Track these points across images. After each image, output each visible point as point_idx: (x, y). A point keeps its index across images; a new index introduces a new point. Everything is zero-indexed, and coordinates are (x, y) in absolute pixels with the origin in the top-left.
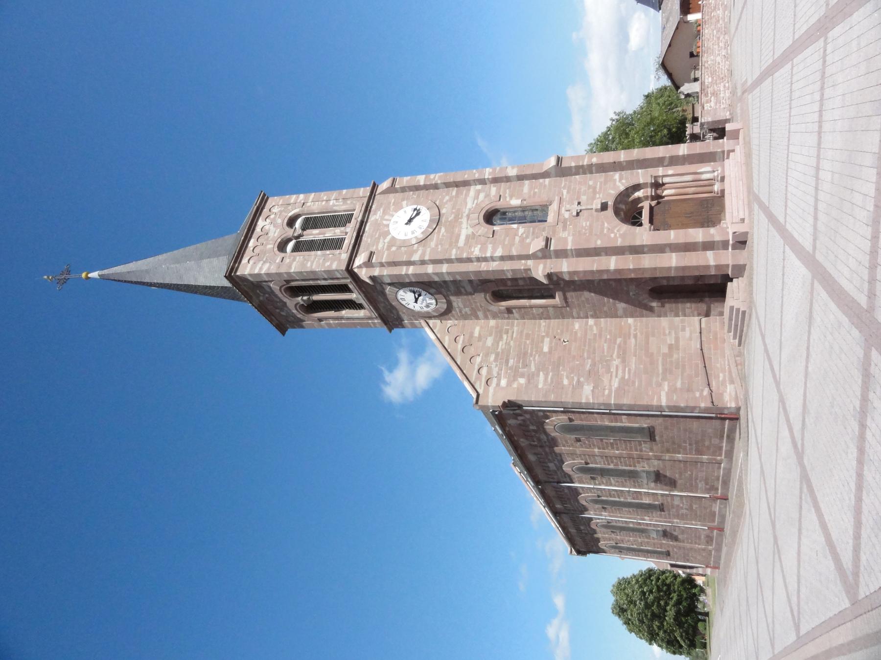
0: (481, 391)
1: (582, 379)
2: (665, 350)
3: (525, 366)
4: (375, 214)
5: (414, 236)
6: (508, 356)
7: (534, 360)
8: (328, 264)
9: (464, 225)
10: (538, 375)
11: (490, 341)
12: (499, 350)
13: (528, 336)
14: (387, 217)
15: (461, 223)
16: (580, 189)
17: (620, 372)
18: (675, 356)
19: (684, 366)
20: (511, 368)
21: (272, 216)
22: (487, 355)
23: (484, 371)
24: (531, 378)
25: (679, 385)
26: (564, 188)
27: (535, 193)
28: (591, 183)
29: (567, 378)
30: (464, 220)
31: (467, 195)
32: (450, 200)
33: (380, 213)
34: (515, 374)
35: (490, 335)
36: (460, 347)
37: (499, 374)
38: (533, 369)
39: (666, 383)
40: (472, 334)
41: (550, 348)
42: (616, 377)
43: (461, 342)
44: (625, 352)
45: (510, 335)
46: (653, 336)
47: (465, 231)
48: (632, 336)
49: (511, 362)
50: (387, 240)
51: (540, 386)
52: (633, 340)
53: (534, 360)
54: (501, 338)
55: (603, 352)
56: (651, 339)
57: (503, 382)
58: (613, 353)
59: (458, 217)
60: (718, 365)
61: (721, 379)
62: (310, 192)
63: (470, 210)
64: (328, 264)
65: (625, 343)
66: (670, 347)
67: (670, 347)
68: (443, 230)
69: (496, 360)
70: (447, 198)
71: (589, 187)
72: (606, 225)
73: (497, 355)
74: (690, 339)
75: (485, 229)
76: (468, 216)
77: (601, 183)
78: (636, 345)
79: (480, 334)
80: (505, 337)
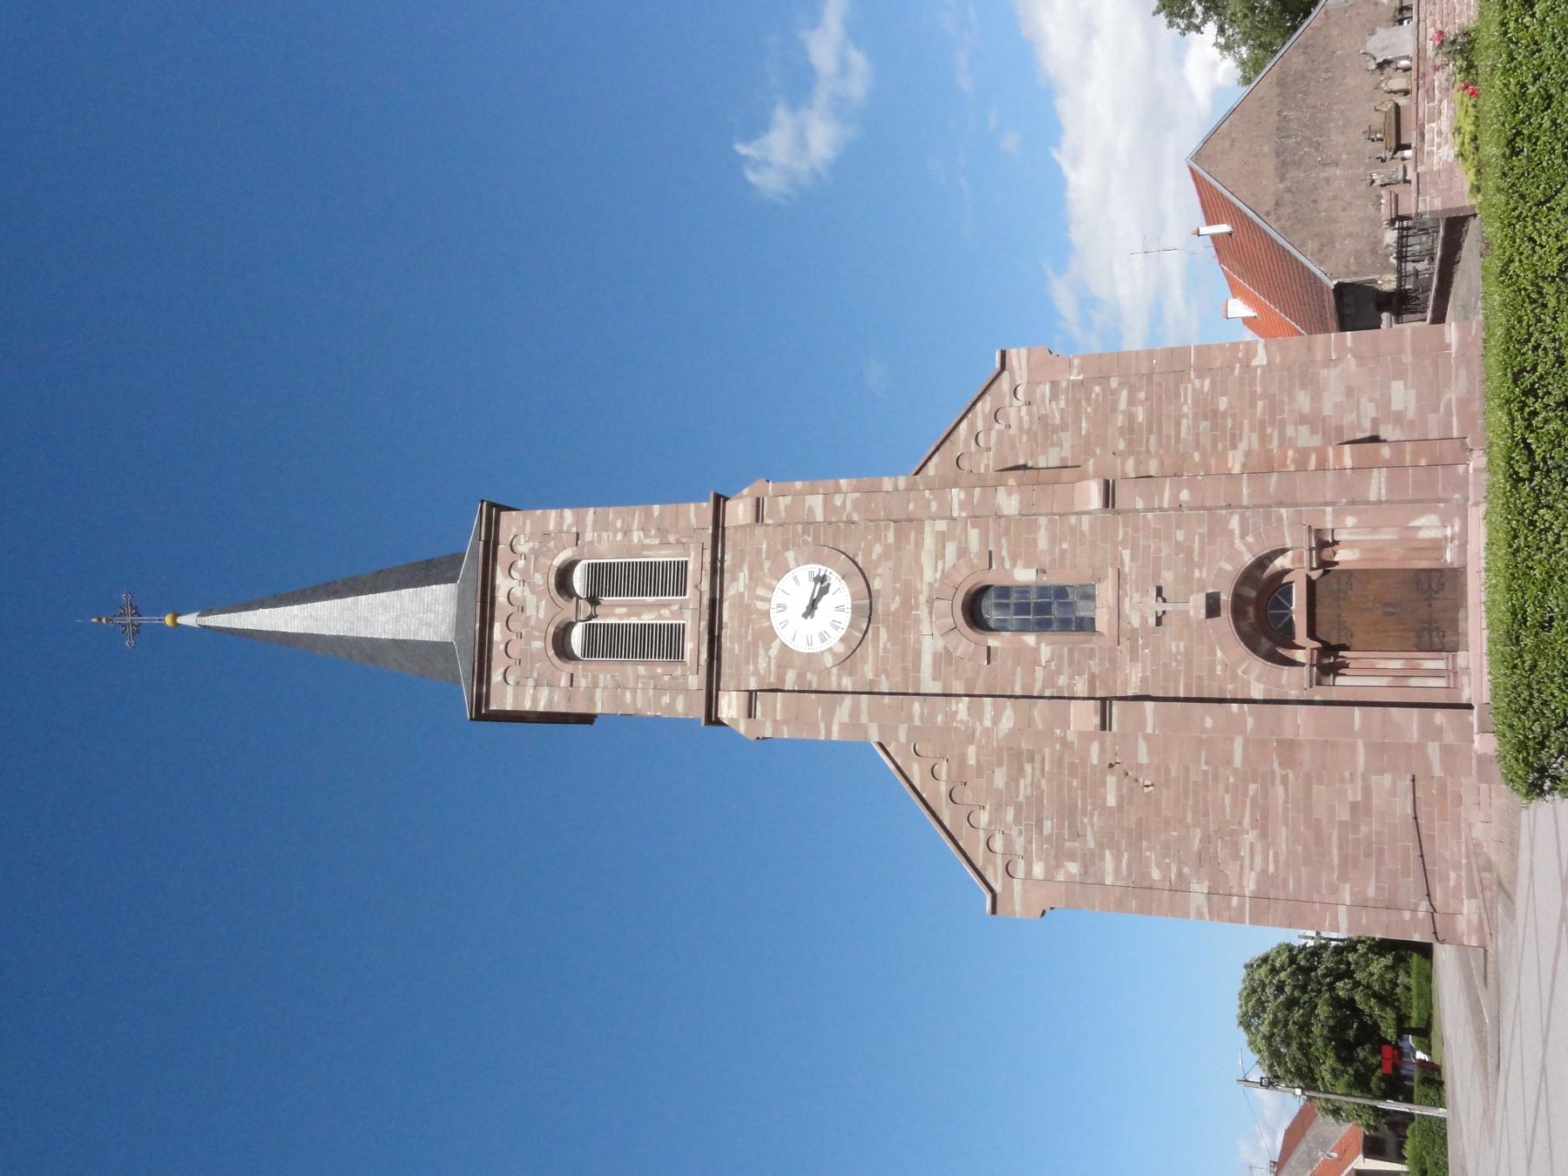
0: (998, 888)
1: (1186, 870)
2: (1344, 815)
3: (1077, 835)
4: (735, 579)
5: (825, 646)
6: (1039, 813)
7: (1092, 825)
8: (666, 699)
9: (925, 628)
10: (1102, 858)
11: (1000, 778)
12: (1021, 798)
13: (1072, 766)
14: (760, 592)
15: (918, 621)
16: (1158, 550)
17: (1258, 859)
18: (1364, 829)
19: (1381, 852)
20: (1048, 840)
21: (521, 563)
22: (998, 808)
23: (998, 844)
24: (1089, 862)
25: (1371, 892)
26: (1124, 543)
27: (1063, 552)
28: (1180, 535)
29: (1158, 867)
30: (923, 612)
31: (919, 545)
32: (885, 555)
33: (743, 576)
34: (1058, 857)
35: (1000, 765)
36: (943, 788)
37: (1027, 851)
38: (1091, 844)
39: (1348, 886)
40: (963, 759)
41: (1120, 799)
42: (1252, 869)
43: (944, 776)
44: (1265, 817)
45: (1037, 765)
46: (1320, 782)
47: (930, 646)
48: (1278, 781)
49: (1047, 825)
50: (774, 652)
51: (1109, 881)
52: (1280, 790)
53: (1092, 825)
54: (1021, 770)
55: (1224, 813)
56: (1315, 787)
57: (1038, 870)
58: (1243, 817)
59: (908, 605)
60: (1447, 854)
61: (1452, 883)
62: (587, 505)
63: (931, 585)
64: (666, 699)
65: (1265, 793)
66: (1354, 807)
67: (1354, 807)
68: (883, 635)
69: (1017, 820)
70: (878, 549)
71: (1179, 547)
72: (1219, 654)
73: (1018, 809)
74: (1393, 792)
75: (967, 642)
76: (930, 602)
77: (1202, 536)
78: (1286, 802)
79: (978, 761)
80: (1028, 768)
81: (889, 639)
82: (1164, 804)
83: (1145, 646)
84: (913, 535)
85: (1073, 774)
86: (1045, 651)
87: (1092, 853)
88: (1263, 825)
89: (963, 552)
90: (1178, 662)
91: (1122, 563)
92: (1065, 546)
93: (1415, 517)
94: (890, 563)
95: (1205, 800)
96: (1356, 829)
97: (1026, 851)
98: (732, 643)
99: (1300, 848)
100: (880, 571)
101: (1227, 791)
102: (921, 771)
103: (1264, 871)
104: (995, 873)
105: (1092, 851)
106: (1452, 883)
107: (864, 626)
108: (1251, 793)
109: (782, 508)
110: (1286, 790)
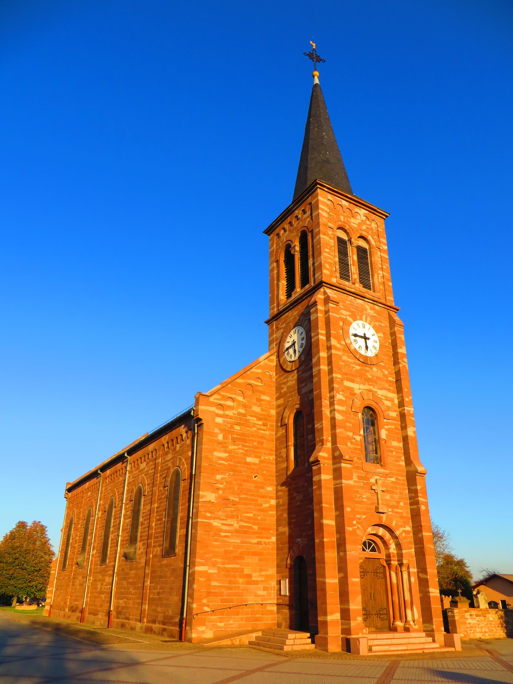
0: (212, 399)
1: (221, 492)
2: (246, 571)
3: (234, 441)
4: (371, 309)
5: (353, 342)
6: (243, 425)
7: (239, 449)
8: (328, 266)
9: (362, 387)
10: (225, 452)
11: (256, 409)
12: (249, 417)
13: (262, 443)
14: (368, 319)
15: (364, 384)
16: (396, 493)
17: (227, 528)
18: (240, 580)
19: (230, 588)
20: (232, 427)
21: (368, 222)
22: (244, 406)
23: (229, 403)
24: (223, 445)
25: (213, 583)
26: (397, 479)
27: (392, 452)
28: (402, 504)
29: (222, 478)
30: (366, 387)
31: (389, 390)
32: (384, 375)
33: (372, 312)
34: (227, 431)
35: (262, 410)
36: (252, 382)
37: (227, 416)
38: (231, 447)
39: (216, 571)
40: (264, 393)
41: (249, 464)
42: (223, 524)
43: (256, 383)
44: (245, 532)
45: (262, 427)
46: (260, 560)
47: (357, 387)
48: (260, 540)
49: (237, 428)
50: (349, 318)
51: (215, 453)
52: (255, 541)
53: (239, 449)
54: (260, 419)
55: (245, 513)
56: (257, 558)
57: (219, 420)
58: (244, 522)
59: (368, 381)
60: (231, 622)
61: (219, 624)
62: (389, 254)
63: (376, 392)
64: (328, 266)
65: (254, 533)
66: (249, 576)
67: (249, 576)
68: (358, 368)
69: (240, 414)
70: (386, 373)
71: (398, 503)
72: (364, 517)
73: (244, 415)
74: (256, 595)
75: (359, 404)
76: (370, 390)
77: (402, 513)
78: (251, 543)
79: (263, 400)
80: (261, 423)
81: (357, 369)
82: (249, 484)
83: (364, 483)
84: (392, 388)
85: (259, 442)
86: (358, 438)
87: (226, 447)
88: (242, 532)
89: (389, 409)
90: (360, 497)
91: (391, 477)
92: (394, 453)
93: (417, 608)
94: (382, 376)
95: (251, 504)
96: (241, 577)
97: (227, 415)
98: (350, 301)
99: (231, 549)
100: (379, 371)
101: (254, 515)
102: (258, 373)
103: (222, 531)
104: (217, 399)
105: (228, 446)
106: (219, 624)
107: (361, 360)
108: (254, 527)
109: (401, 336)
110: (255, 544)
